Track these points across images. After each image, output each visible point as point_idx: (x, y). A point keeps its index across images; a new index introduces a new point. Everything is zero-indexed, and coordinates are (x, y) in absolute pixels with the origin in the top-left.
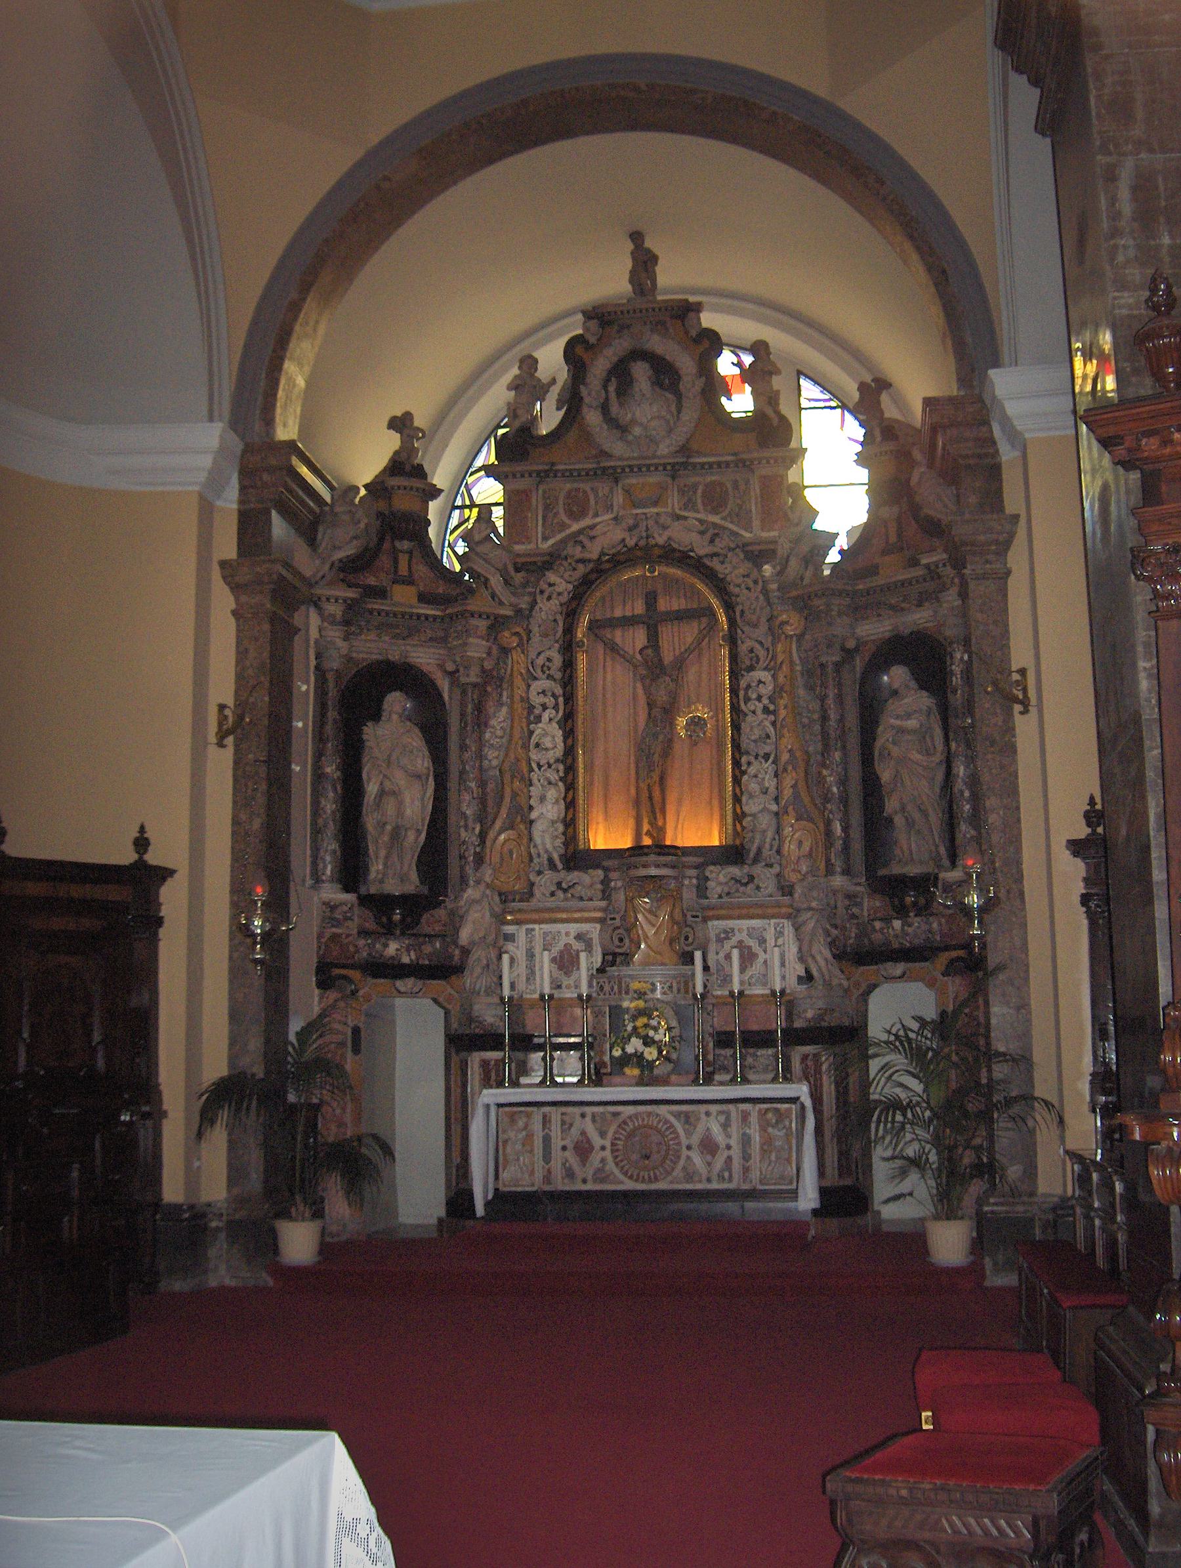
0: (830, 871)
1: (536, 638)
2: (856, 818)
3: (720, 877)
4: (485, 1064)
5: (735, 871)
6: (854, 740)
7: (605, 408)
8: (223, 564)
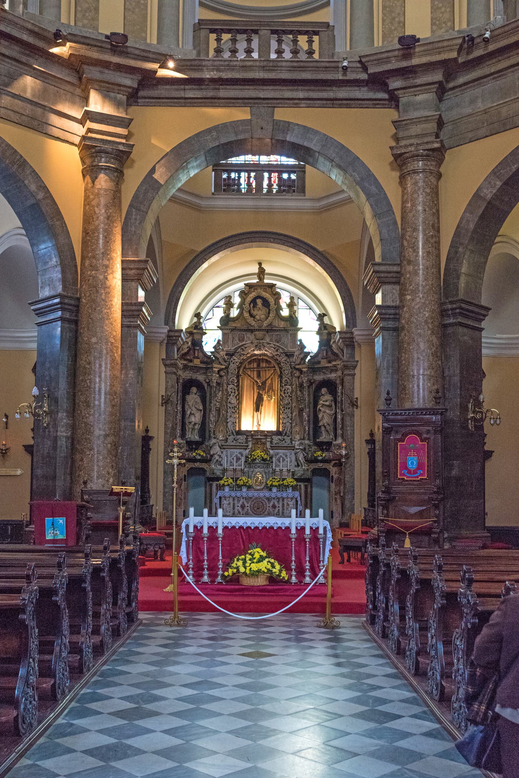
0: (304, 439)
1: (230, 374)
2: (312, 426)
3: (276, 439)
4: (217, 485)
5: (280, 437)
6: (312, 405)
7: (250, 312)
8: (163, 359)
